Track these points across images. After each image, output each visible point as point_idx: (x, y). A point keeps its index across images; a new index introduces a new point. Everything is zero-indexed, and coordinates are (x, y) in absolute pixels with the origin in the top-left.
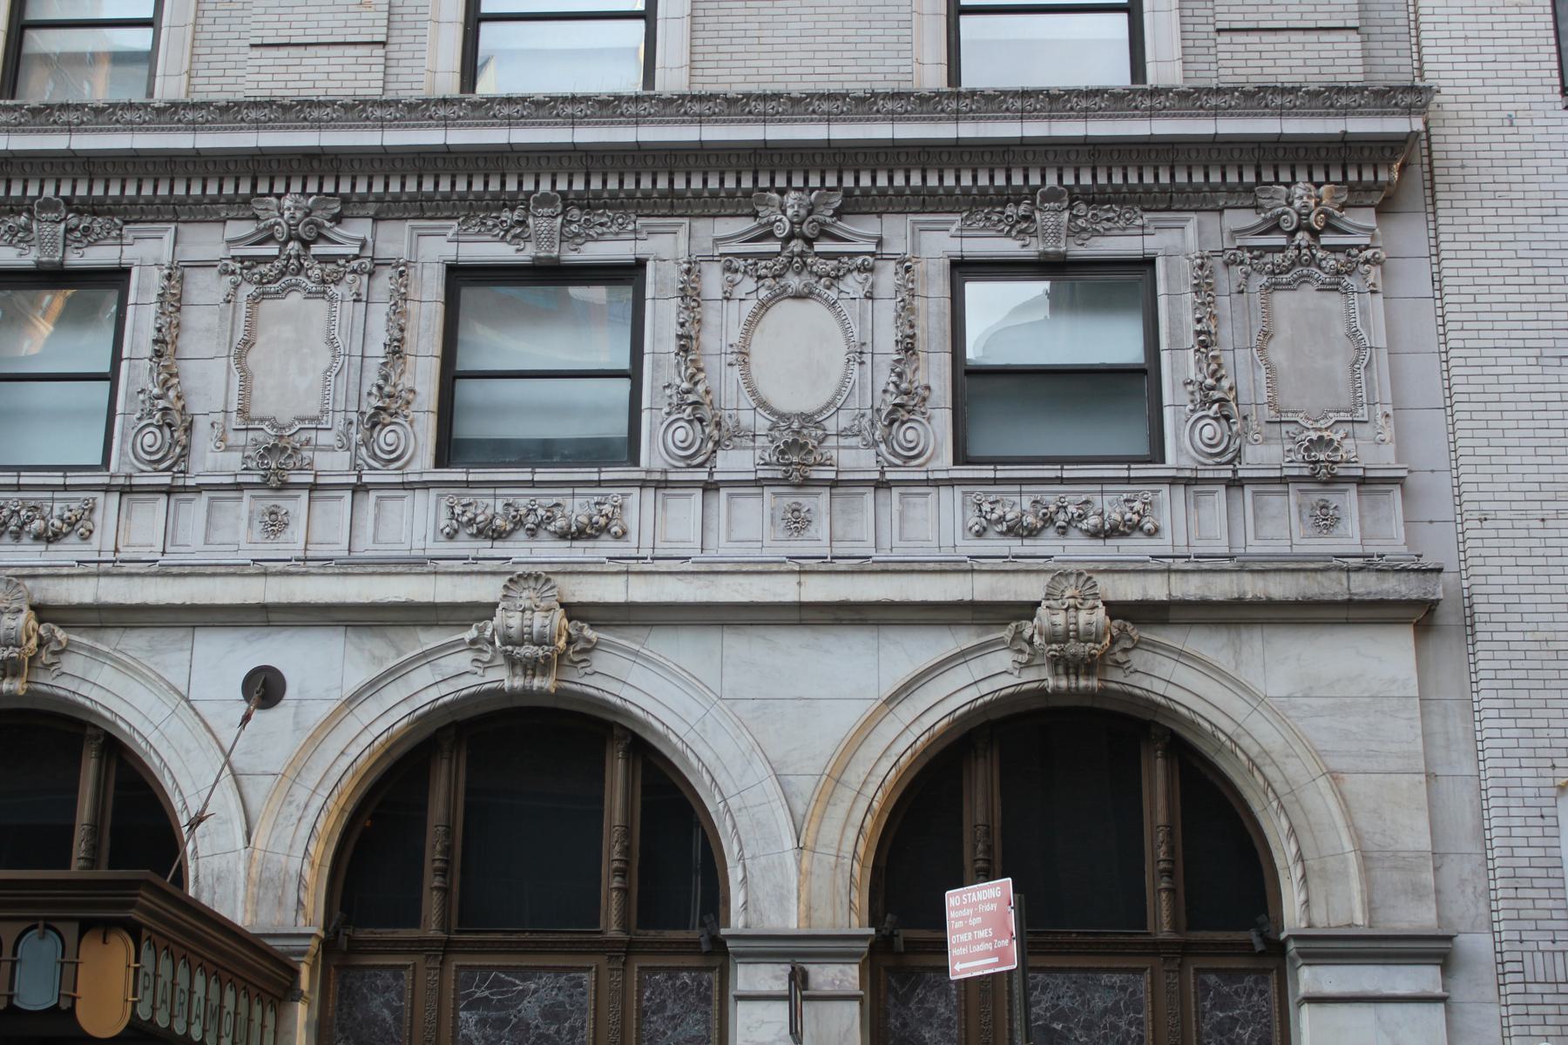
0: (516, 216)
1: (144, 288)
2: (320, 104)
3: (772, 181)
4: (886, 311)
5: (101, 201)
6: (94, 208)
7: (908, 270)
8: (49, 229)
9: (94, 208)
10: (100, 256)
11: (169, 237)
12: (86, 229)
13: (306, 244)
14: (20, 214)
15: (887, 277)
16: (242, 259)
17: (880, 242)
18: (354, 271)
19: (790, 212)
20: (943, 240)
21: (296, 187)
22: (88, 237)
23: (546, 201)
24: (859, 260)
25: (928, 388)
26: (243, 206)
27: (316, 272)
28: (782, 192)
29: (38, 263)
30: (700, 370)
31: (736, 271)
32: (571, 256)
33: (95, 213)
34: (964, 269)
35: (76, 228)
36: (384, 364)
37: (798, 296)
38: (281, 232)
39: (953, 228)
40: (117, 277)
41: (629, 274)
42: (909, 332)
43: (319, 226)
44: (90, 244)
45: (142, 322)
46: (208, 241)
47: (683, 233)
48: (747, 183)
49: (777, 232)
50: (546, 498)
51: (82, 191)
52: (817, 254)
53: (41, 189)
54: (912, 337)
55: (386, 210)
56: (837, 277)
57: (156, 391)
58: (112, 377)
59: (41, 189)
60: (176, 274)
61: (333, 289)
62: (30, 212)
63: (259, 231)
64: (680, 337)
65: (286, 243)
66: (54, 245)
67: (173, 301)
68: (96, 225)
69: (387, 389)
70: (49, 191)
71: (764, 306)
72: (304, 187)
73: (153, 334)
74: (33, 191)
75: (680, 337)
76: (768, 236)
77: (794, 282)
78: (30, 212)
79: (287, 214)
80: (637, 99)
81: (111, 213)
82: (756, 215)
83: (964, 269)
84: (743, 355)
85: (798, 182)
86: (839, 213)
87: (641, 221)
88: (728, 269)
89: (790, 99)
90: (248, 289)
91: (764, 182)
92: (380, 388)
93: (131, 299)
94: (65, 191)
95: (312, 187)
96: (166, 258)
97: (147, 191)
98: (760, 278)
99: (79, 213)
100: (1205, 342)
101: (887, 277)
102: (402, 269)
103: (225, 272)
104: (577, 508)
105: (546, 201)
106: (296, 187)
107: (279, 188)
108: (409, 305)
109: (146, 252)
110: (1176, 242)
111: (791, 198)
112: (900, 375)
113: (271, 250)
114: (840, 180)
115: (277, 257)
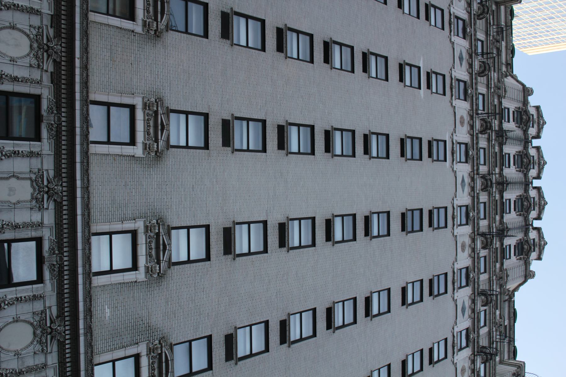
1: (35, 146)
2: (91, 301)
3: (64, 182)
5: (61, 133)
6: (61, 271)
7: (43, 368)
8: (54, 260)
9: (61, 271)
10: (45, 133)
11: (50, 152)
12: (52, 130)
13: (47, 193)
14: (57, 111)
17: (47, 209)
18: (40, 207)
19: (59, 328)
20: (47, 235)
21: (63, 49)
22: (50, 130)
24: (45, 349)
25: (4, 233)
26: (61, 314)
28: (61, 185)
29: (43, 116)
30: (8, 157)
31: (41, 314)
33: (57, 131)
34: (39, 241)
35: (55, 267)
36: (12, 224)
38: (50, 186)
39: (51, 237)
40: (38, 138)
41: (38, 138)
42: (21, 227)
43: (52, 196)
44: (48, 130)
45: (24, 146)
46: (47, 21)
47: (50, 152)
49: (52, 325)
51: (63, 128)
52: (43, 195)
53: (64, 117)
54: (20, 228)
56: (40, 343)
57: (4, 153)
58: (8, 137)
59: (64, 117)
60: (38, 155)
61: (34, 202)
62: (59, 254)
63: (51, 179)
64: (21, 297)
65: (47, 186)
66: (48, 120)
67: (31, 155)
68: (53, 132)
69: (5, 226)
70: (63, 119)
72: (64, 191)
73: (21, 150)
74: (63, 114)
75: (21, 297)
76: (49, 182)
78: (59, 254)
79: (56, 187)
80: (89, 230)
81: (59, 274)
82: (57, 317)
83: (39, 241)
84: (16, 320)
85: (67, 328)
86: (58, 340)
87: (55, 280)
88: (42, 312)
89: (88, 187)
90: (33, 177)
91: (64, 180)
92: (4, 74)
93: (31, 143)
94: (64, 124)
95: (65, 194)
96: (44, 152)
97: (63, 86)
98: (40, 322)
99: (57, 127)
103: (39, 170)
106: (65, 189)
107: (63, 45)
108: (30, 228)
109: (45, 146)
111: (62, 328)
112: (8, 225)
113: (45, 183)
114: (68, 339)
115: (43, 184)
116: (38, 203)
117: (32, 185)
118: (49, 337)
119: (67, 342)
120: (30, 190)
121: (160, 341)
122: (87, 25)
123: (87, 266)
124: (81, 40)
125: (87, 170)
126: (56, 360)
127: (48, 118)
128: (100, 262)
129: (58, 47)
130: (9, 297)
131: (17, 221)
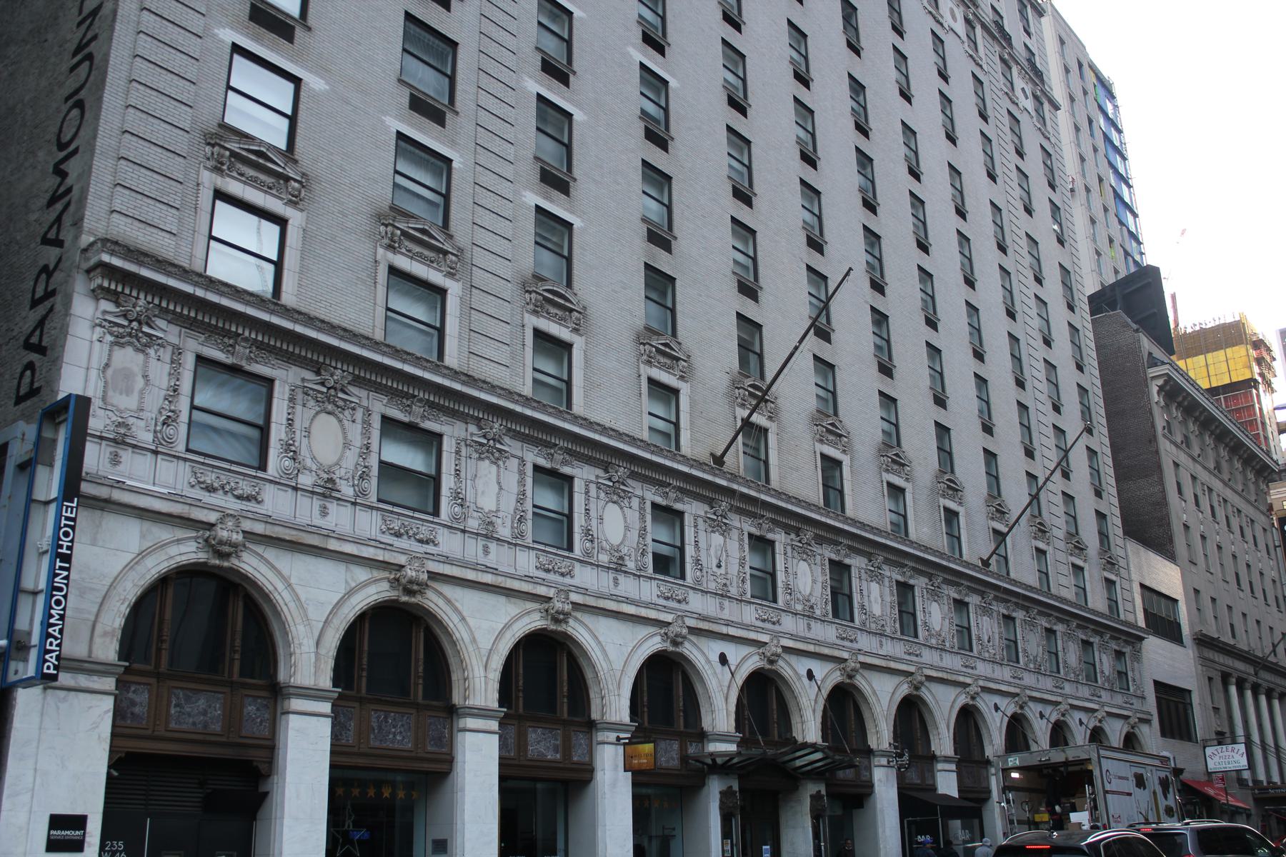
0: (231, 342)
4: (358, 427)
15: (359, 414)
16: (110, 322)
23: (246, 340)
27: (144, 340)
32: (248, 368)
37: (329, 413)
48: (120, 289)
50: (233, 479)
55: (177, 319)
71: (317, 413)
77: (330, 407)
100: (457, 473)
101: (359, 414)
102: (178, 351)
104: (245, 487)
105: (246, 340)
110: (452, 432)
116: (145, 344)
117: (122, 345)
118: (341, 395)
119: (178, 310)
120: (129, 350)
121: (209, 144)
122: (388, 346)
123: (170, 269)
124: (169, 274)
125: (493, 387)
126: (174, 329)
127: (240, 356)
128: (256, 279)
129: (338, 374)
130: (283, 436)
131: (165, 385)
